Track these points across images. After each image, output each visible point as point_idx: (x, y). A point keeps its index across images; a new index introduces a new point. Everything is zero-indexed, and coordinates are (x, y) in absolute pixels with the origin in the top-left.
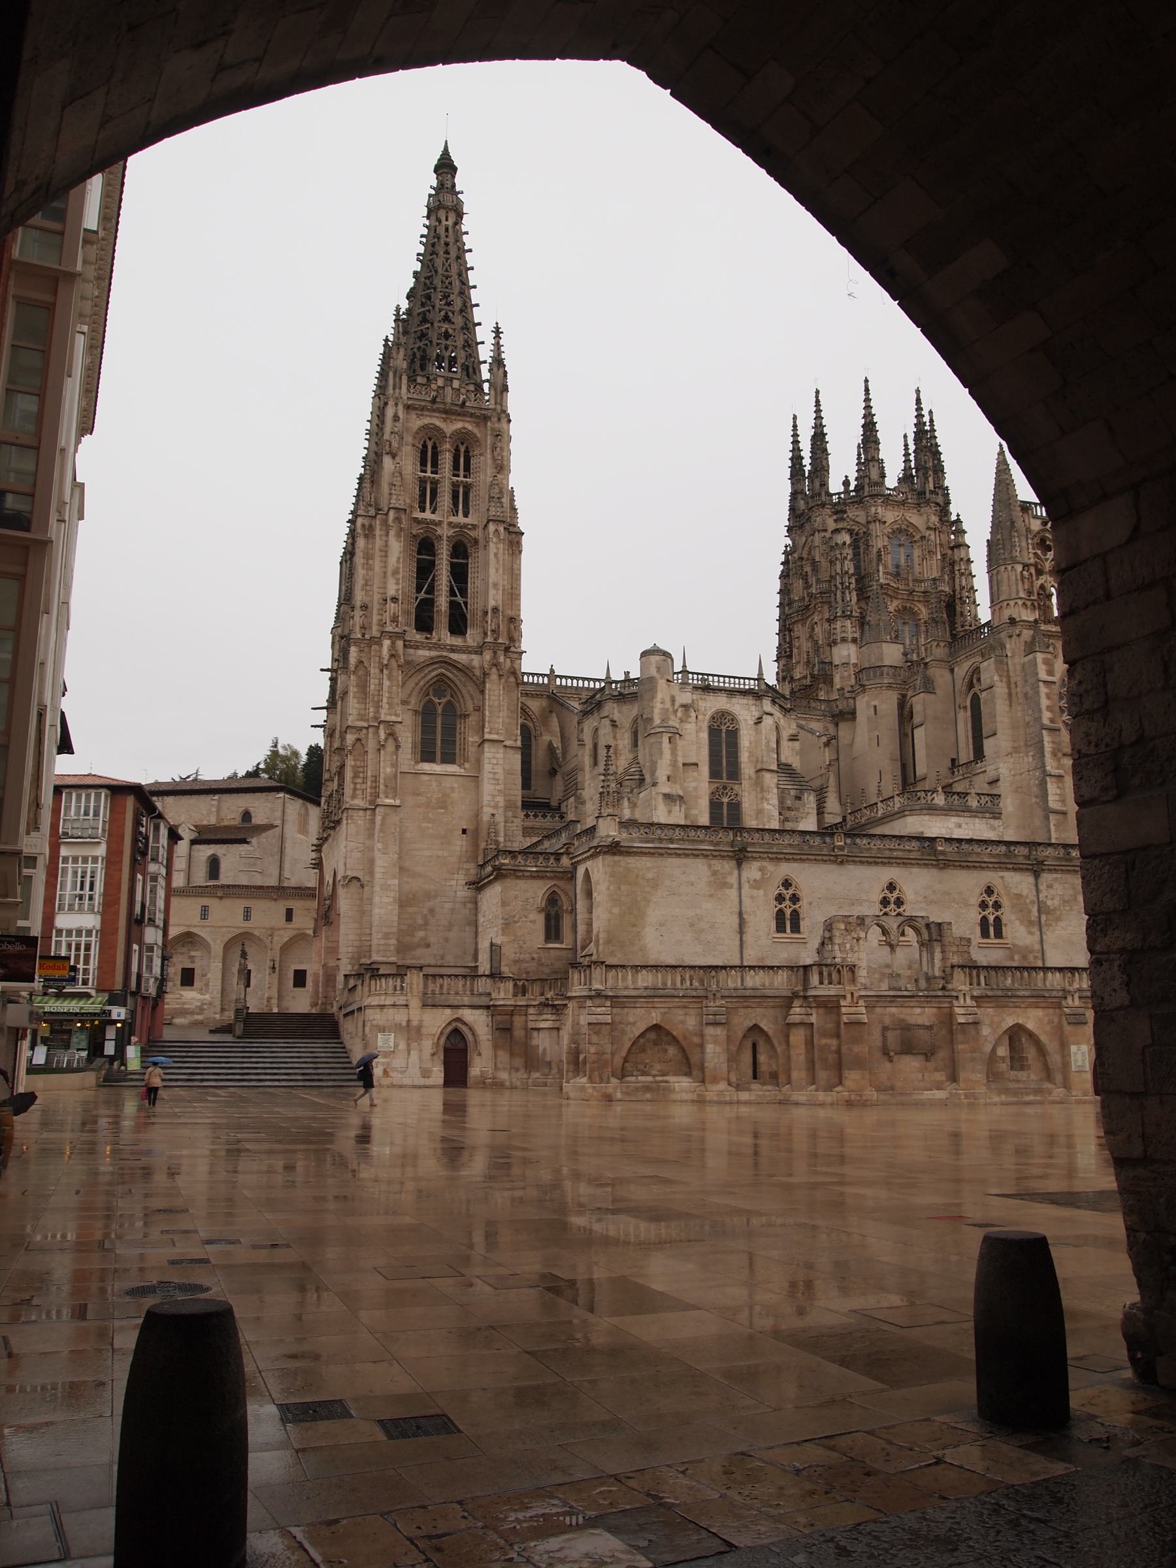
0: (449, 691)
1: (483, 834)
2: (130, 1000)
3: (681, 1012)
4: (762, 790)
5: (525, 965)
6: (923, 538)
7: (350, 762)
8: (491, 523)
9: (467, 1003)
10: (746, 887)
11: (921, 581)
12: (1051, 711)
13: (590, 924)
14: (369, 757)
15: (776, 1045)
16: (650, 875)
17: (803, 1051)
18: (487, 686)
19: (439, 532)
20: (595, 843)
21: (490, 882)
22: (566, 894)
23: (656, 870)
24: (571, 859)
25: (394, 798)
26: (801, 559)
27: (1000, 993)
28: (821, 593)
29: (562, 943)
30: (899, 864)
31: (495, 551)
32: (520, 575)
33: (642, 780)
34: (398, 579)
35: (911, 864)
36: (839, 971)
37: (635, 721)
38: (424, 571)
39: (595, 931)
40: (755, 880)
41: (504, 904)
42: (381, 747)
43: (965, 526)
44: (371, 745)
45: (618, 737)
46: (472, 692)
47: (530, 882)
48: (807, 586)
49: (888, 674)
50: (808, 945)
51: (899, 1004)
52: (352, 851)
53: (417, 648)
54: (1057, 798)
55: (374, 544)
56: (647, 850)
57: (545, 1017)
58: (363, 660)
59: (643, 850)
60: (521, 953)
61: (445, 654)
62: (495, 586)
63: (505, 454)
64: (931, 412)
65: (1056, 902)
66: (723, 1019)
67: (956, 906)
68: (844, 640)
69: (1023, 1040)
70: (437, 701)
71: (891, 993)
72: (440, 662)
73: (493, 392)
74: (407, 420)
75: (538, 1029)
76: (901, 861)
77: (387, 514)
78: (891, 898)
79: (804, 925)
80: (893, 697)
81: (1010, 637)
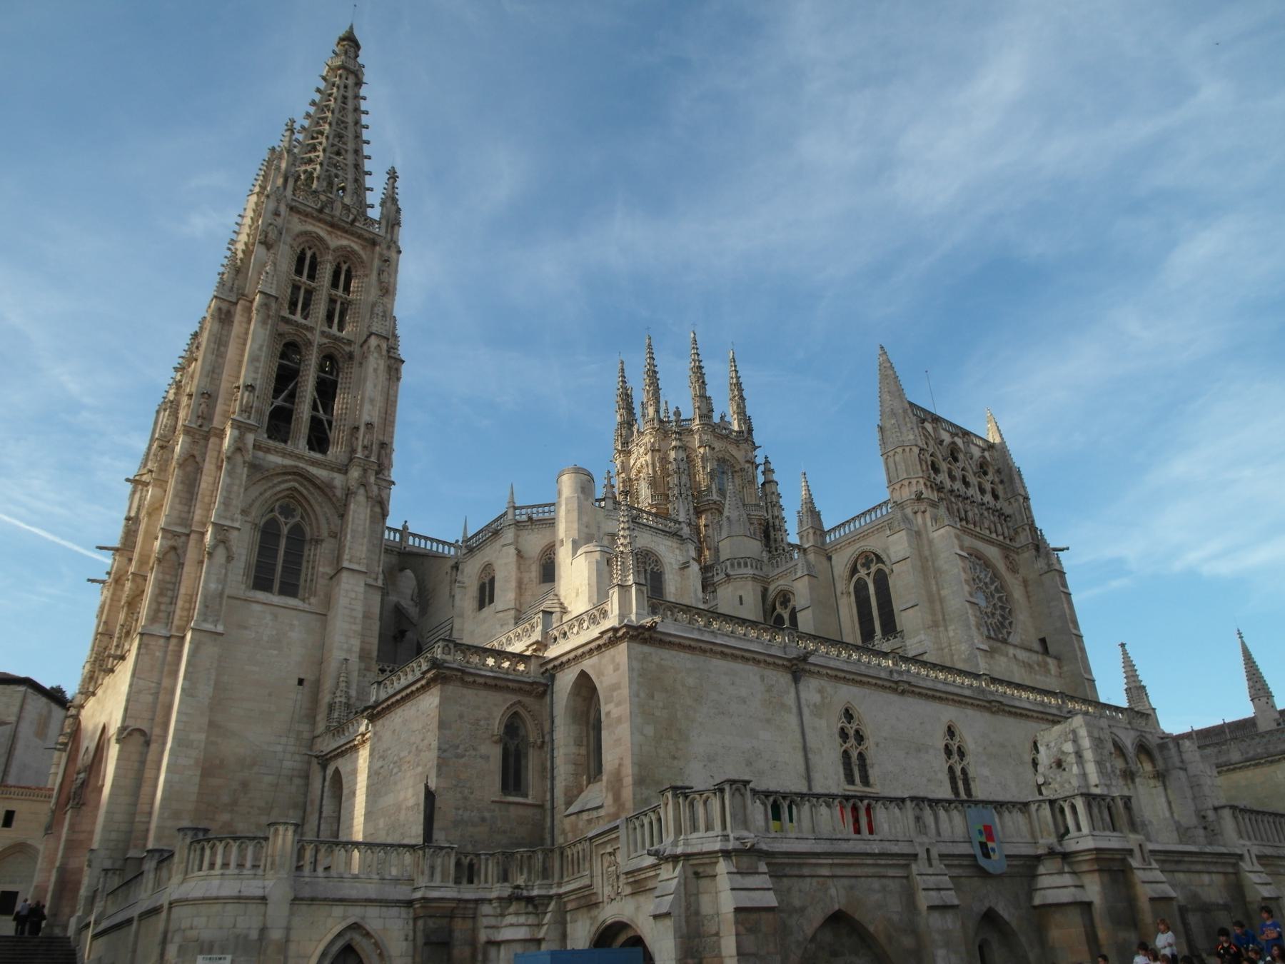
0: (300, 510)
1: (328, 684)
6: (742, 470)
8: (373, 338)
9: (374, 896)
10: (806, 711)
12: (969, 585)
14: (186, 569)
16: (691, 681)
18: (352, 506)
19: (309, 335)
20: (612, 621)
25: (215, 623)
29: (526, 796)
31: (375, 366)
32: (396, 402)
34: (257, 368)
38: (285, 378)
40: (815, 705)
41: (442, 725)
44: (191, 554)
47: (483, 693)
49: (752, 566)
52: (139, 692)
53: (268, 451)
55: (230, 331)
56: (687, 643)
57: (510, 919)
58: (196, 453)
59: (682, 641)
60: (465, 809)
61: (301, 465)
62: (372, 401)
63: (392, 280)
72: (294, 474)
73: (384, 222)
74: (289, 222)
75: (498, 944)
77: (252, 302)
80: (759, 589)
81: (916, 513)
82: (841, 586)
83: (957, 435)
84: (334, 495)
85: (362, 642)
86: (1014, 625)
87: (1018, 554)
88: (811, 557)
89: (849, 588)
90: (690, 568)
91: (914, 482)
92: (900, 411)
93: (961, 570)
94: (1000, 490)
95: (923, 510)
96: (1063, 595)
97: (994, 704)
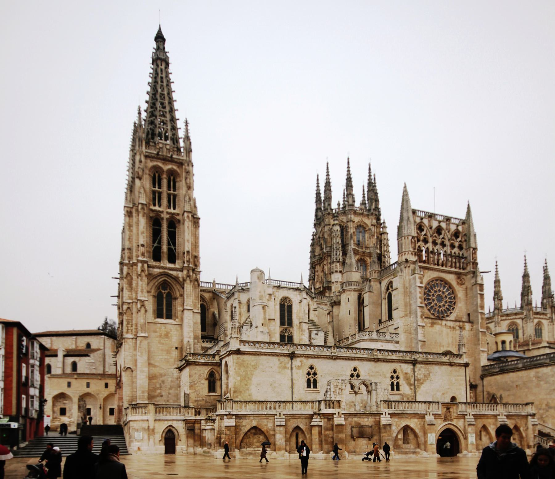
0: (169, 287)
2: (21, 420)
3: (266, 421)
4: (302, 331)
5: (200, 402)
6: (370, 229)
7: (125, 318)
10: (294, 368)
11: (368, 248)
13: (227, 385)
15: (306, 434)
16: (253, 364)
17: (318, 437)
18: (185, 285)
21: (185, 367)
22: (218, 372)
23: (256, 361)
24: (220, 357)
26: (319, 237)
28: (327, 252)
29: (216, 393)
33: (251, 325)
36: (333, 403)
37: (248, 301)
39: (229, 388)
40: (298, 366)
41: (190, 376)
42: (139, 311)
43: (387, 225)
44: (134, 310)
45: (241, 307)
46: (179, 288)
47: (201, 367)
48: (322, 249)
49: (354, 285)
50: (320, 393)
66: (284, 424)
67: (381, 377)
68: (336, 272)
69: (409, 431)
70: (163, 292)
71: (355, 412)
78: (355, 374)
79: (318, 385)
82: (383, 295)
84: (179, 280)
85: (194, 333)
87: (466, 275)
88: (372, 283)
89: (385, 296)
93: (418, 292)
96: (479, 296)
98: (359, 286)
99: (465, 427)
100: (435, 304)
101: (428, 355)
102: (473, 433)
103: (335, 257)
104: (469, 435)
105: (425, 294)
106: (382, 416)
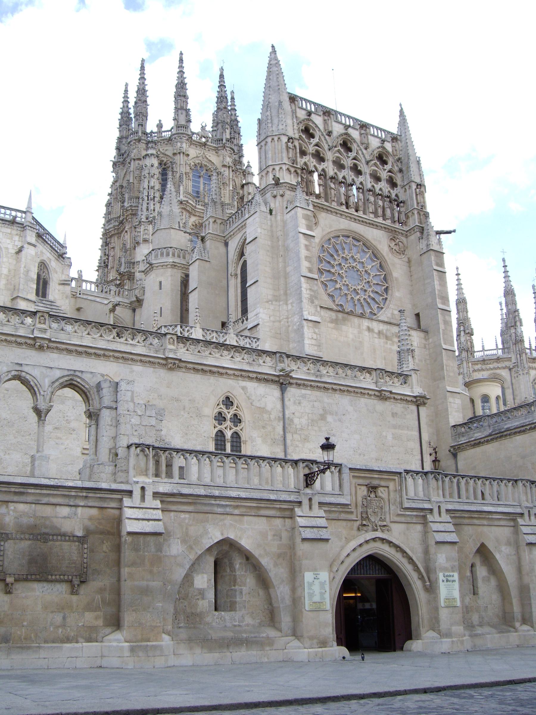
12: (310, 262)
26: (122, 187)
27: (201, 491)
28: (131, 206)
30: (118, 358)
35: (132, 360)
49: (174, 255)
51: (30, 499)
54: (314, 342)
64: (232, 92)
65: (304, 421)
67: (186, 415)
69: (237, 566)
76: (120, 355)
80: (178, 275)
81: (275, 197)
82: (231, 269)
83: (353, 128)
86: (388, 302)
88: (208, 243)
89: (237, 271)
90: (23, 252)
91: (277, 168)
92: (277, 104)
94: (398, 179)
95: (281, 192)
96: (435, 273)
97: (169, 361)
98: (184, 258)
99: (426, 552)
100: (344, 285)
101: (322, 368)
102: (453, 570)
103: (145, 213)
104: (441, 576)
105: (320, 260)
106: (127, 501)
